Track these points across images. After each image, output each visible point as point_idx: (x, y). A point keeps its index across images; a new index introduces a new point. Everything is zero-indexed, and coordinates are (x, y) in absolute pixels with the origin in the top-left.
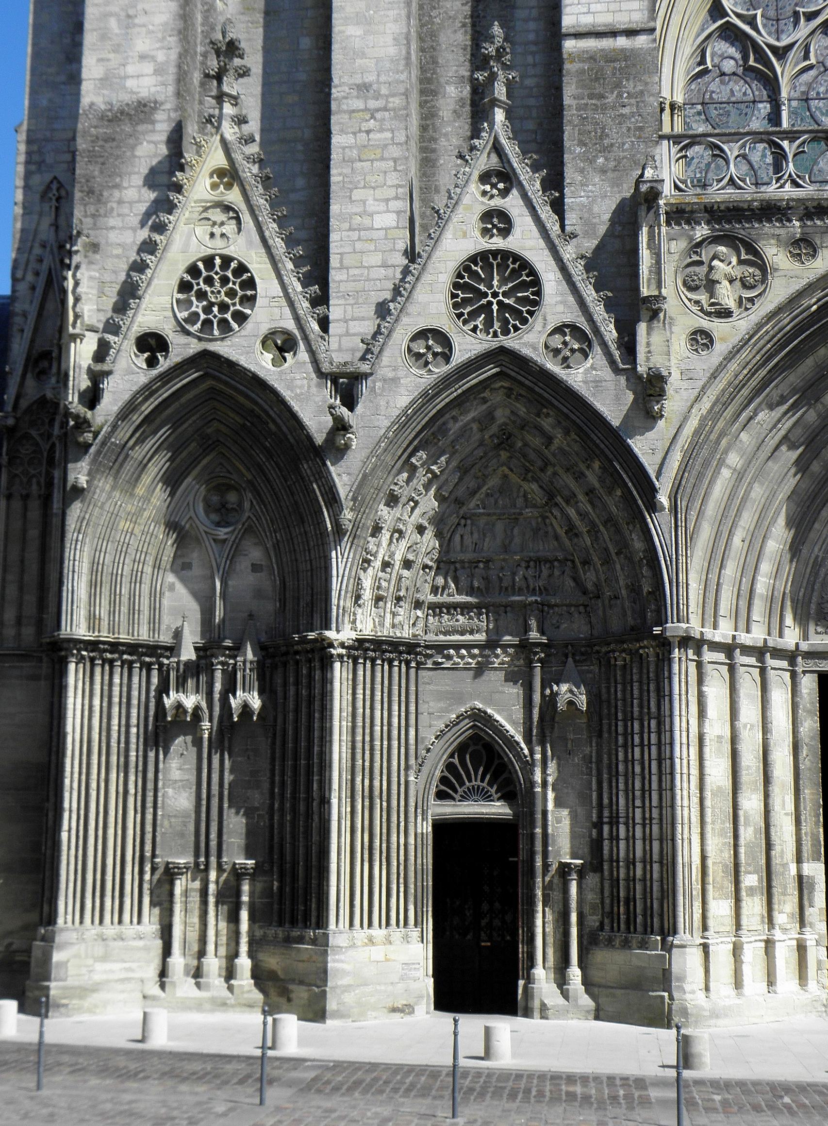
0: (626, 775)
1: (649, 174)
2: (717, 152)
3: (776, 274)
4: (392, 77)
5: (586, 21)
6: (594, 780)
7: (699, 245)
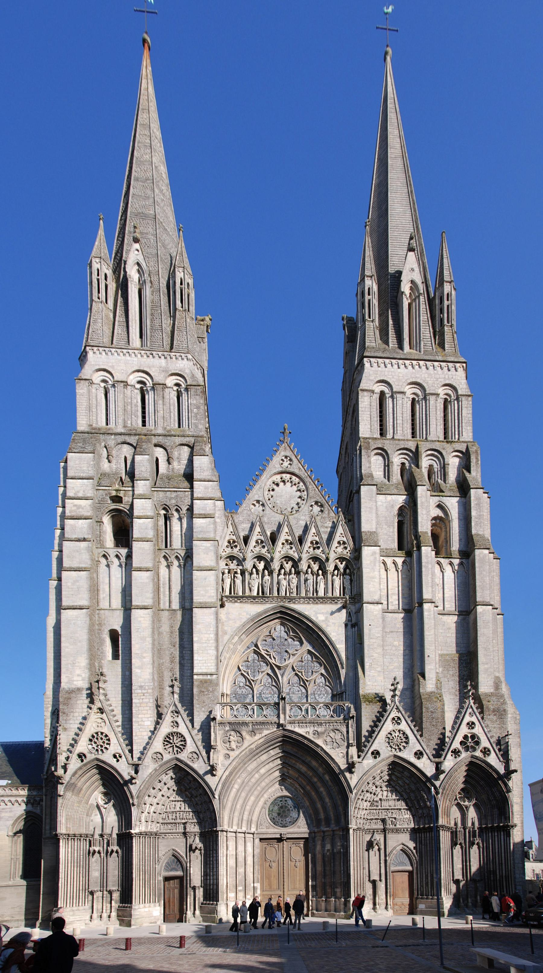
4: (149, 684)
5: (200, 671)
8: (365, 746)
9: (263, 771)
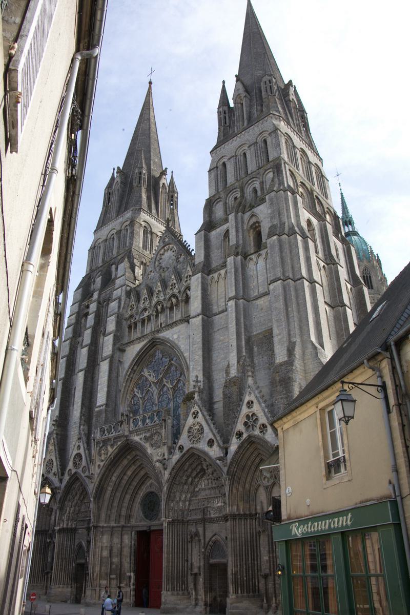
9: (129, 473)
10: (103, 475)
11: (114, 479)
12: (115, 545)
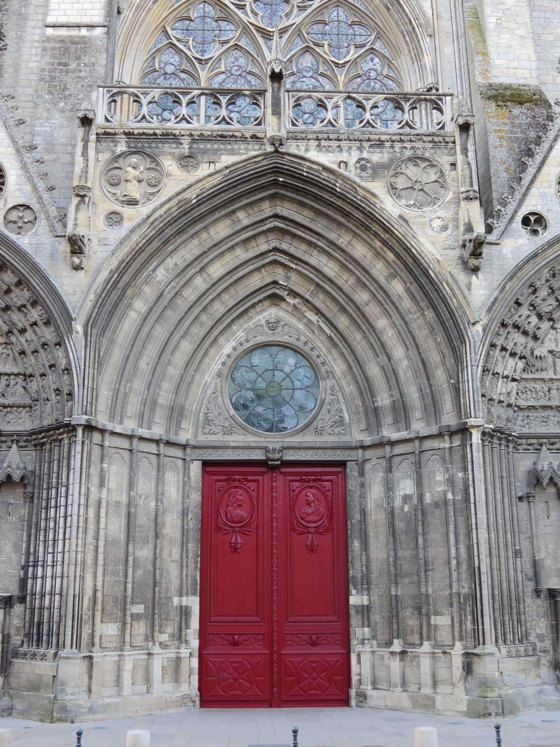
0: (45, 530)
1: (85, 105)
2: (136, 99)
3: (170, 178)
6: (25, 534)
7: (120, 156)
8: (504, 204)
9: (217, 270)
10: (140, 251)
11: (161, 274)
12: (142, 501)
